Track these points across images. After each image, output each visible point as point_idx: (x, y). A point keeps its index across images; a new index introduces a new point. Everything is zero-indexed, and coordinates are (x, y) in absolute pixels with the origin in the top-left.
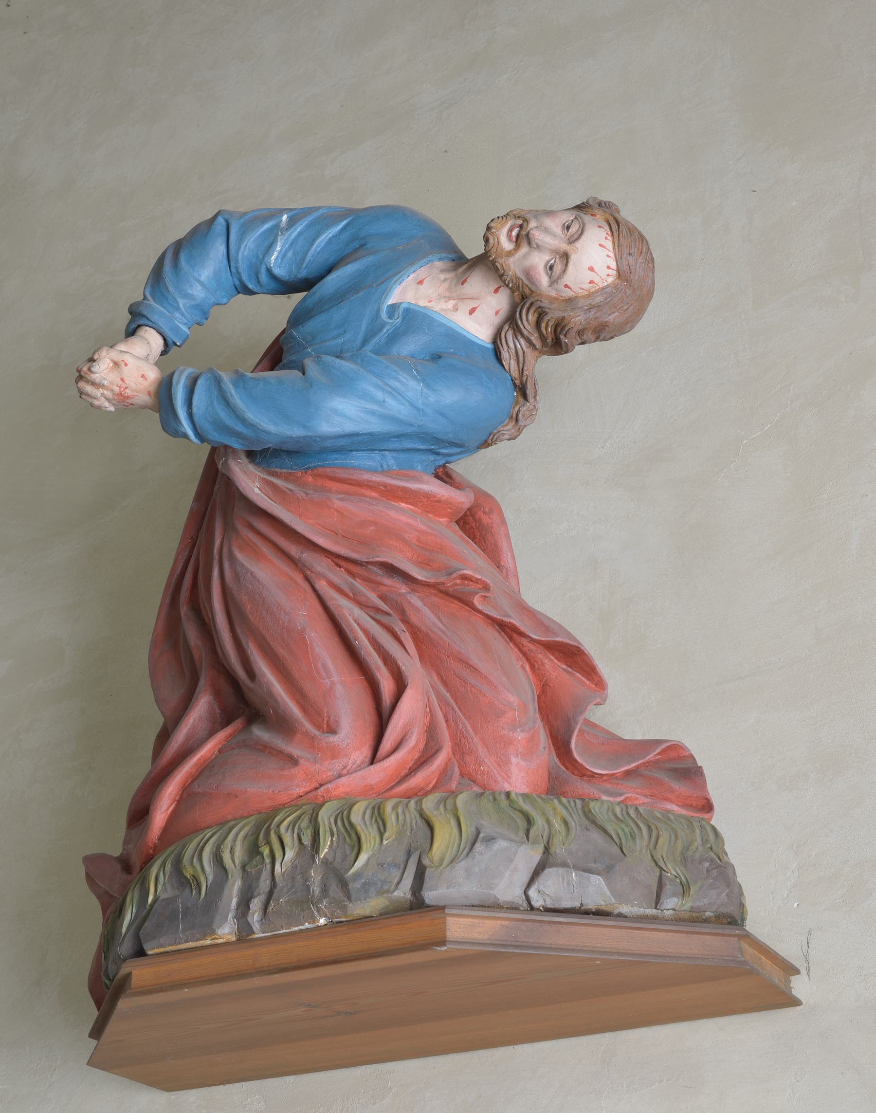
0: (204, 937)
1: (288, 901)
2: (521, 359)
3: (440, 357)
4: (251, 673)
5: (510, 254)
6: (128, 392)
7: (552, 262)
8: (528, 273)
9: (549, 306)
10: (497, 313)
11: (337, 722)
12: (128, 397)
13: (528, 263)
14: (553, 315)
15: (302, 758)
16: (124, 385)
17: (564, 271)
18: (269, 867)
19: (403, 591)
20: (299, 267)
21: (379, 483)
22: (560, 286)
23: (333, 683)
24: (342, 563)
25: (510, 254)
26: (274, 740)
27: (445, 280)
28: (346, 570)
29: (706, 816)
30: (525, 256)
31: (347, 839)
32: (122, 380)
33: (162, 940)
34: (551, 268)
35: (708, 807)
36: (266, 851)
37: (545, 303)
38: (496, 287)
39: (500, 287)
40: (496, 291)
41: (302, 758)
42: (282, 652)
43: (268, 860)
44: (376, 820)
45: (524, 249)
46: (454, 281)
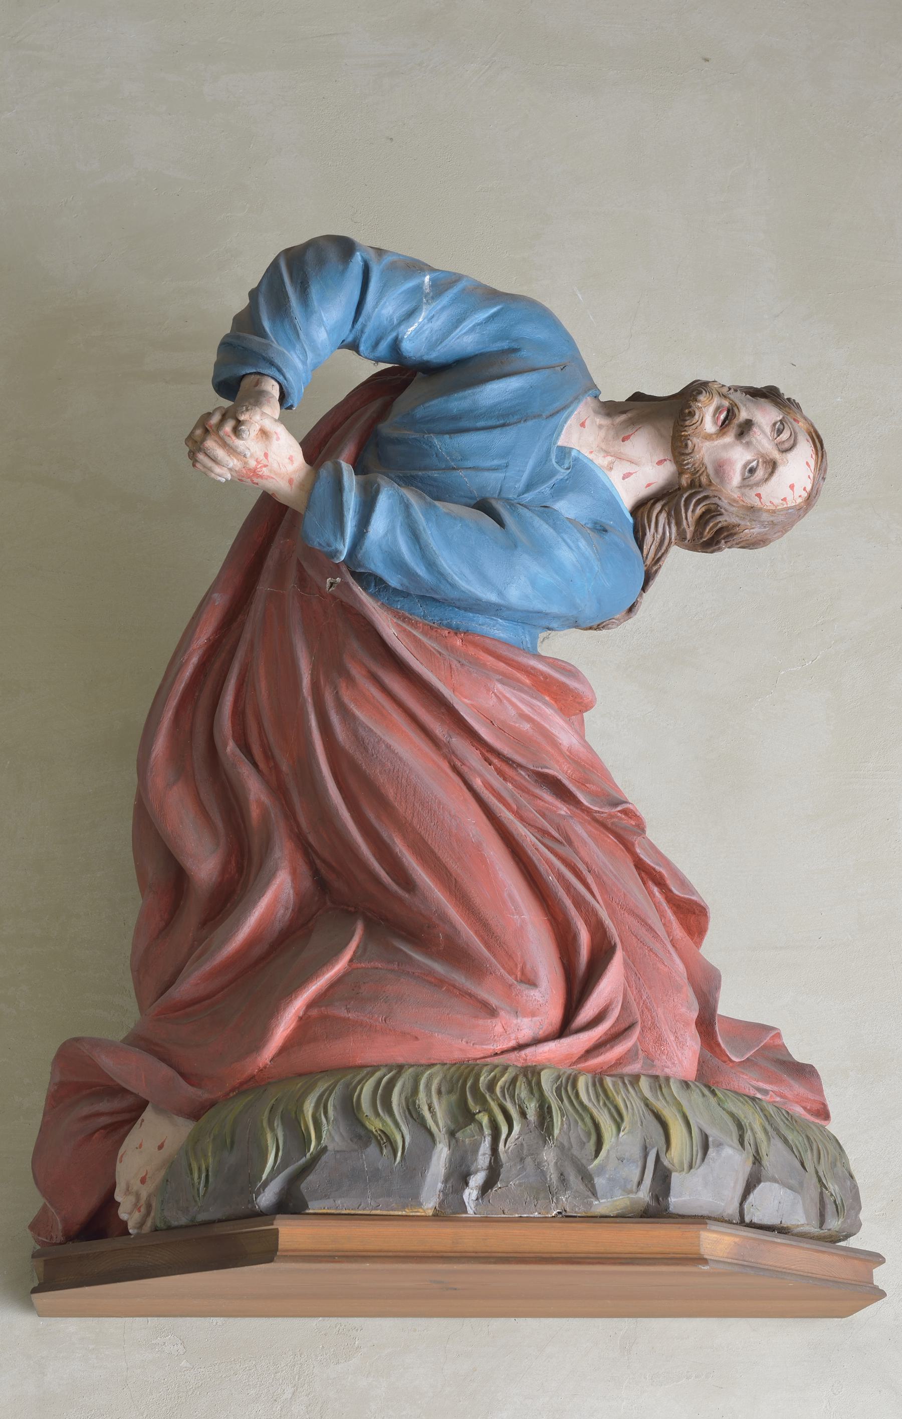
0: (403, 1208)
1: (520, 1185)
2: (664, 548)
3: (606, 531)
4: (407, 882)
5: (709, 437)
6: (265, 471)
7: (754, 464)
8: (720, 468)
9: (727, 507)
10: (648, 485)
11: (536, 973)
12: (261, 477)
13: (725, 455)
14: (724, 520)
15: (502, 1009)
16: (265, 462)
17: (767, 480)
18: (488, 1139)
19: (563, 813)
20: (433, 346)
21: (542, 673)
22: (752, 493)
23: (523, 921)
24: (495, 761)
25: (709, 437)
26: (453, 975)
27: (600, 427)
28: (497, 769)
29: (823, 1123)
30: (725, 447)
31: (580, 1123)
32: (266, 455)
33: (339, 1202)
34: (752, 471)
35: (823, 1113)
36: (484, 1119)
37: (724, 503)
38: (662, 458)
39: (665, 460)
40: (660, 463)
41: (502, 1009)
42: (454, 866)
43: (487, 1131)
44: (605, 1104)
45: (729, 438)
46: (612, 433)
